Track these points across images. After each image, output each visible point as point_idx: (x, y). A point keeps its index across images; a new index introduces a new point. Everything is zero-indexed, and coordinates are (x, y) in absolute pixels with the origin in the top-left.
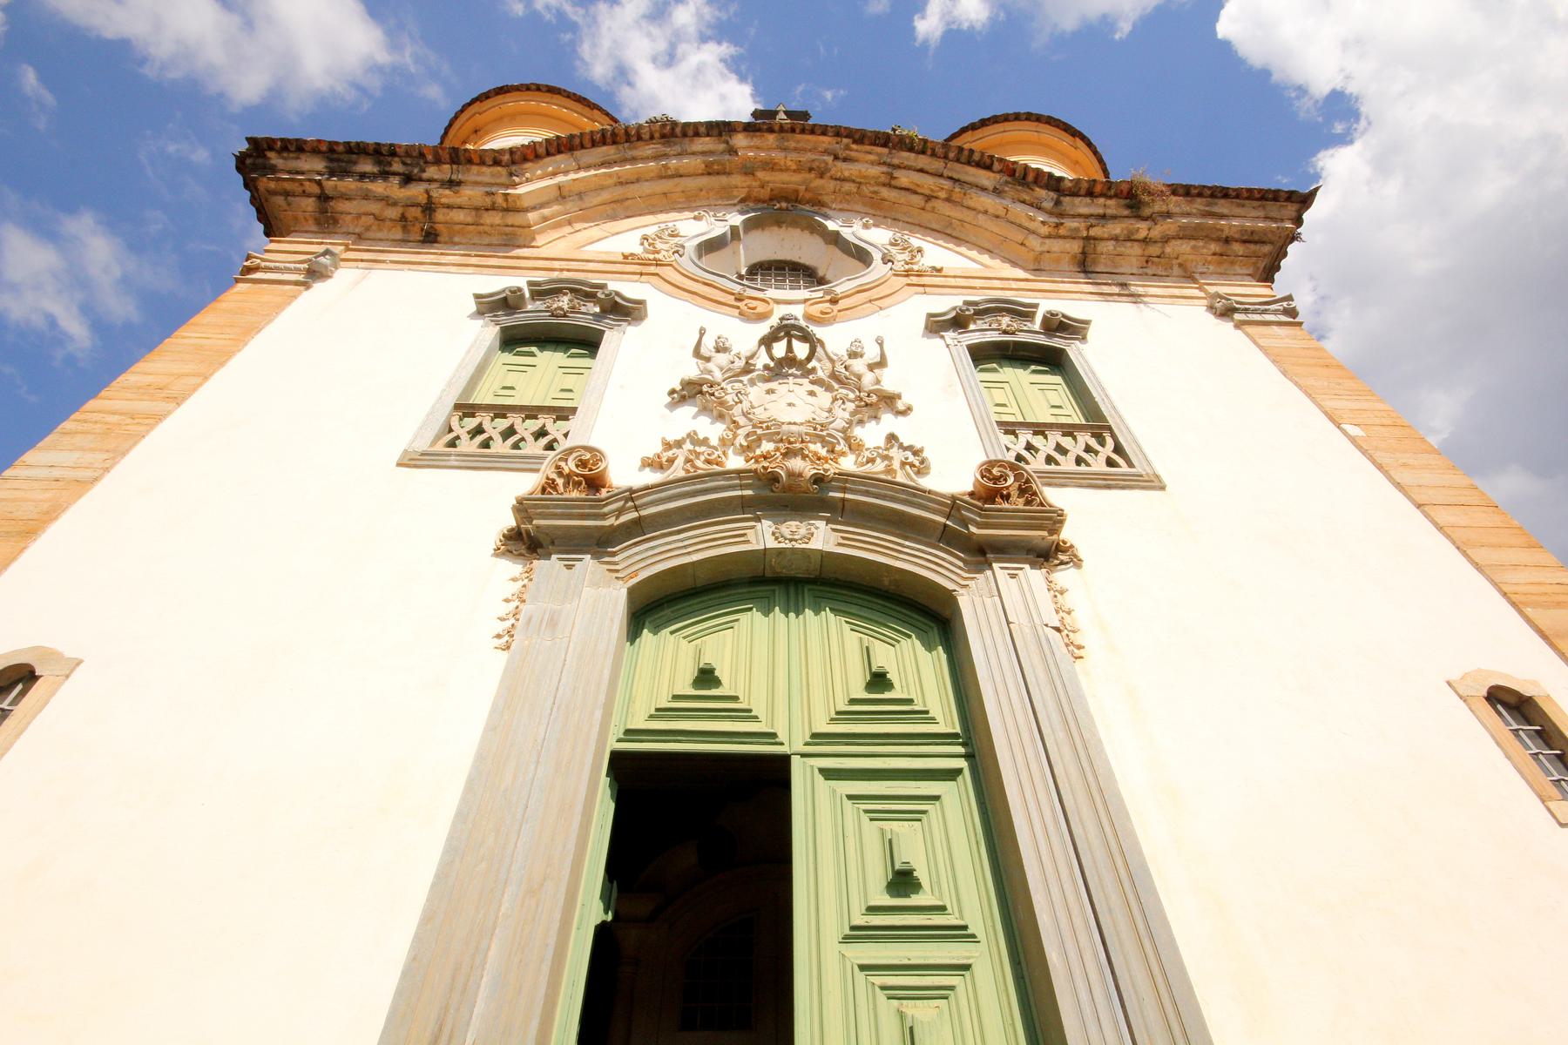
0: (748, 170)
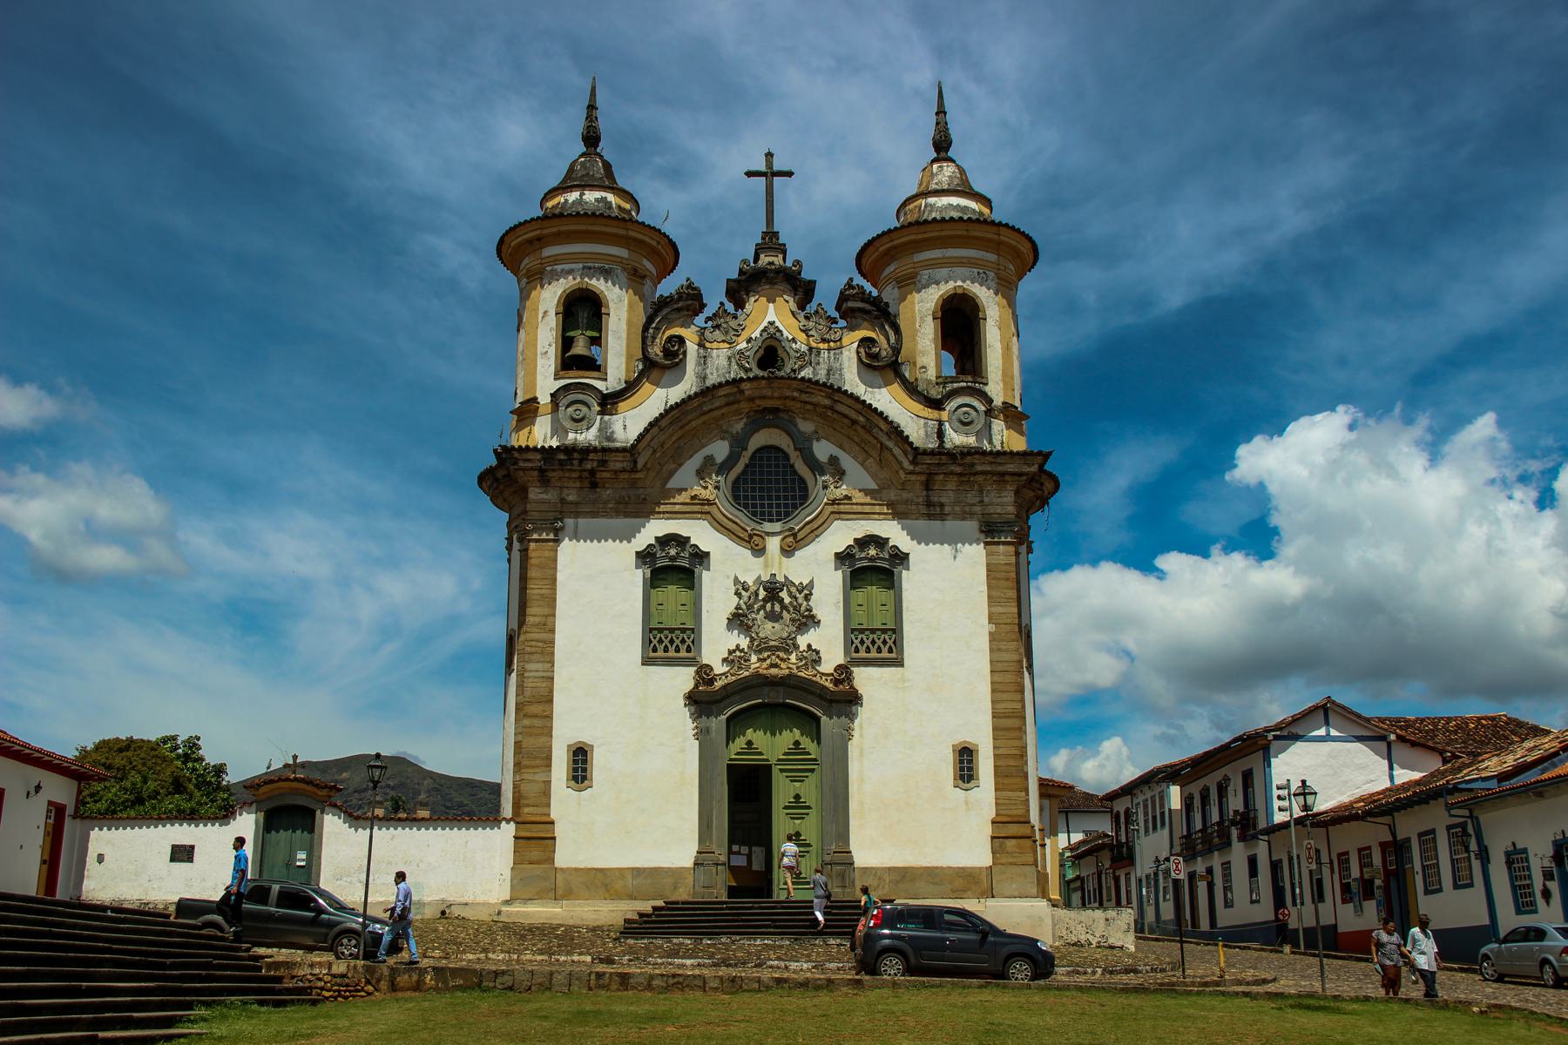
0: (752, 399)
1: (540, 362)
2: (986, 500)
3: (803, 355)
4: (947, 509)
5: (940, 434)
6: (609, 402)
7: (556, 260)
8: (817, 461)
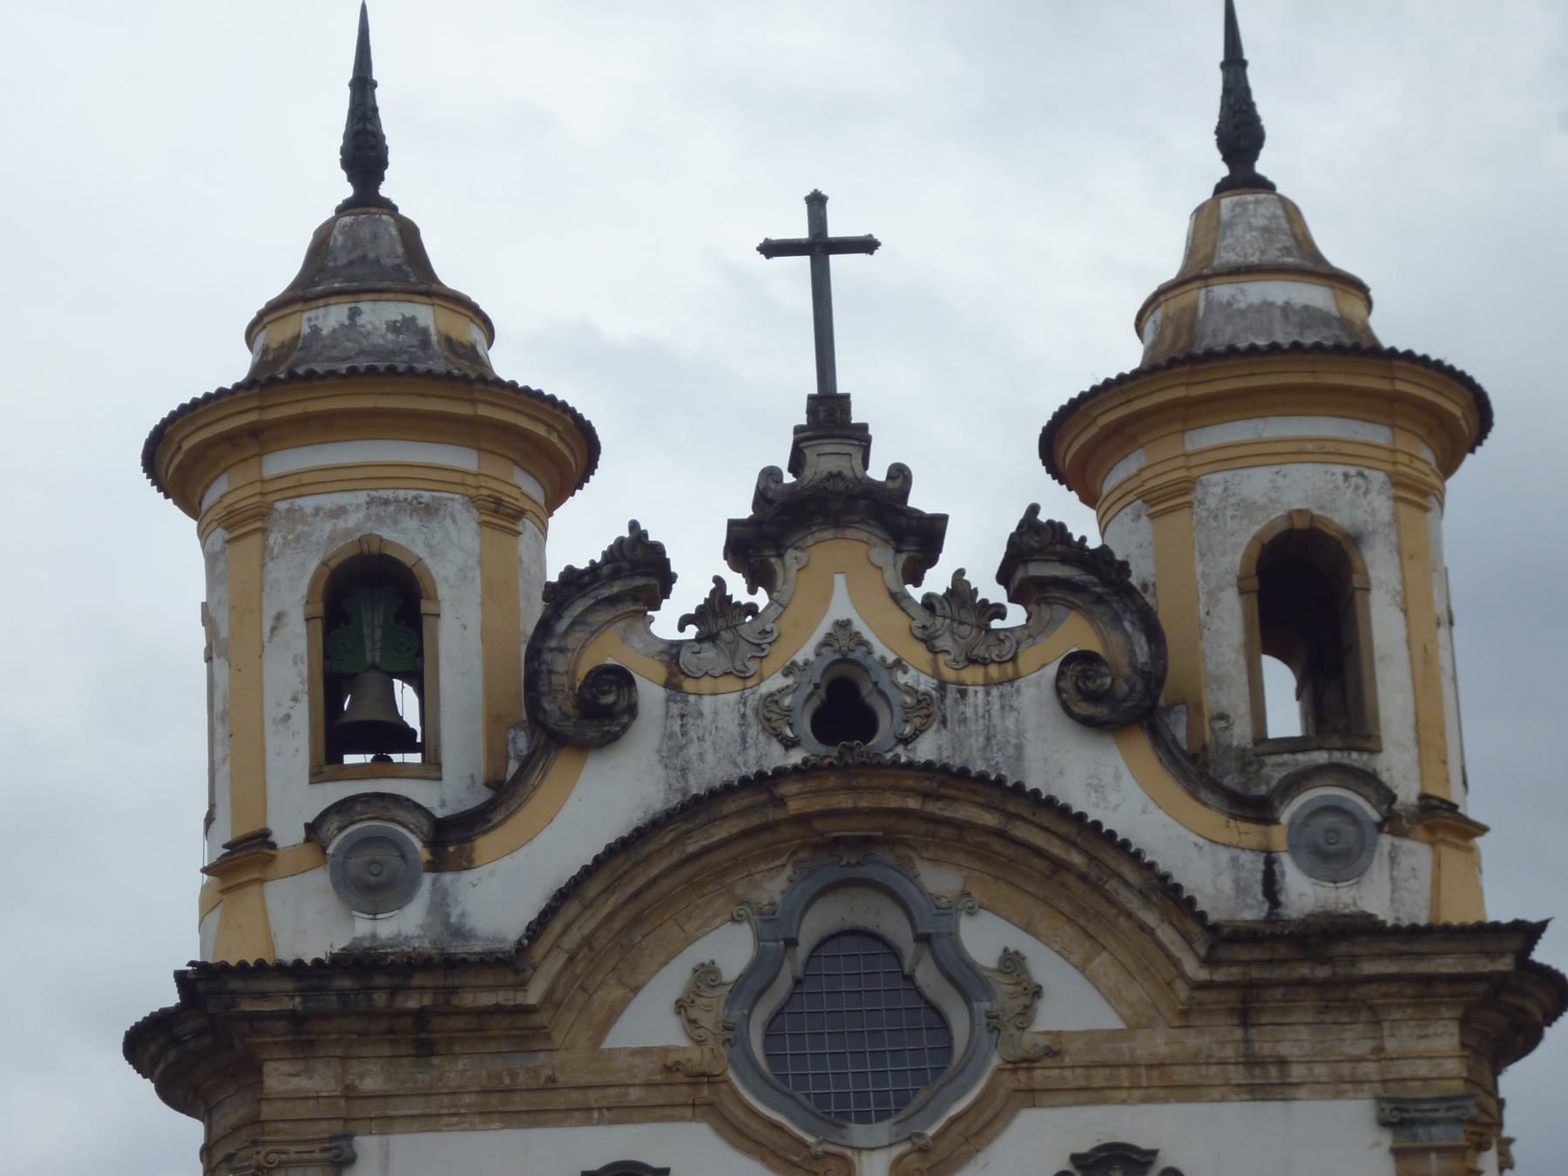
0: (803, 819)
1: (273, 742)
2: (1391, 1045)
3: (923, 701)
4: (1296, 1072)
5: (1271, 885)
6: (453, 839)
7: (300, 484)
8: (970, 966)
